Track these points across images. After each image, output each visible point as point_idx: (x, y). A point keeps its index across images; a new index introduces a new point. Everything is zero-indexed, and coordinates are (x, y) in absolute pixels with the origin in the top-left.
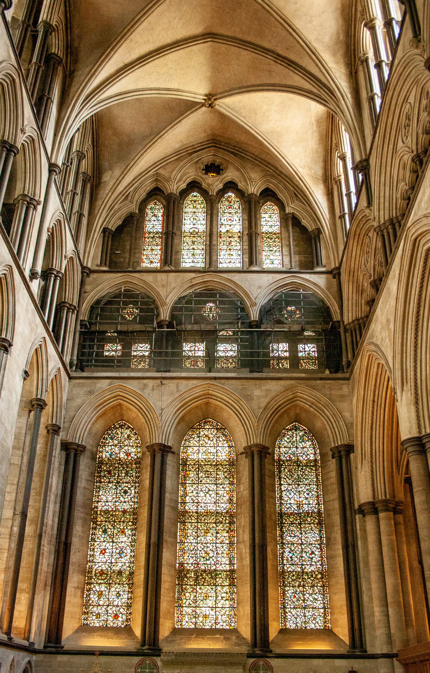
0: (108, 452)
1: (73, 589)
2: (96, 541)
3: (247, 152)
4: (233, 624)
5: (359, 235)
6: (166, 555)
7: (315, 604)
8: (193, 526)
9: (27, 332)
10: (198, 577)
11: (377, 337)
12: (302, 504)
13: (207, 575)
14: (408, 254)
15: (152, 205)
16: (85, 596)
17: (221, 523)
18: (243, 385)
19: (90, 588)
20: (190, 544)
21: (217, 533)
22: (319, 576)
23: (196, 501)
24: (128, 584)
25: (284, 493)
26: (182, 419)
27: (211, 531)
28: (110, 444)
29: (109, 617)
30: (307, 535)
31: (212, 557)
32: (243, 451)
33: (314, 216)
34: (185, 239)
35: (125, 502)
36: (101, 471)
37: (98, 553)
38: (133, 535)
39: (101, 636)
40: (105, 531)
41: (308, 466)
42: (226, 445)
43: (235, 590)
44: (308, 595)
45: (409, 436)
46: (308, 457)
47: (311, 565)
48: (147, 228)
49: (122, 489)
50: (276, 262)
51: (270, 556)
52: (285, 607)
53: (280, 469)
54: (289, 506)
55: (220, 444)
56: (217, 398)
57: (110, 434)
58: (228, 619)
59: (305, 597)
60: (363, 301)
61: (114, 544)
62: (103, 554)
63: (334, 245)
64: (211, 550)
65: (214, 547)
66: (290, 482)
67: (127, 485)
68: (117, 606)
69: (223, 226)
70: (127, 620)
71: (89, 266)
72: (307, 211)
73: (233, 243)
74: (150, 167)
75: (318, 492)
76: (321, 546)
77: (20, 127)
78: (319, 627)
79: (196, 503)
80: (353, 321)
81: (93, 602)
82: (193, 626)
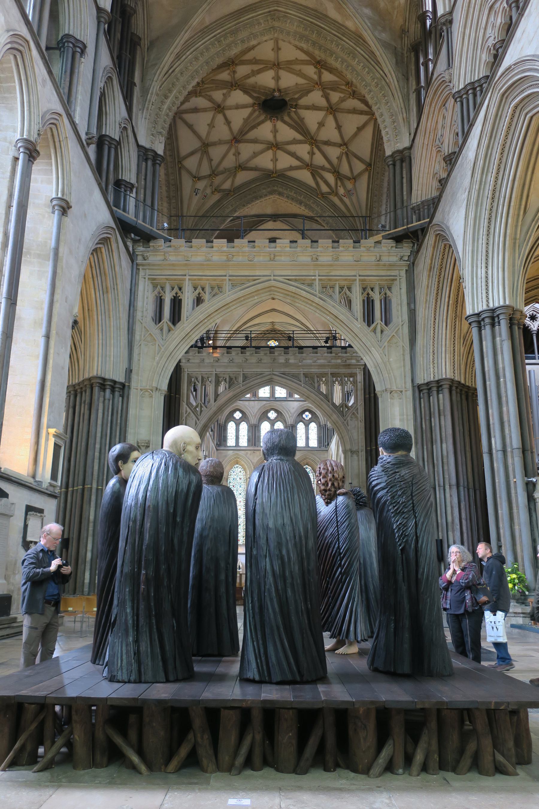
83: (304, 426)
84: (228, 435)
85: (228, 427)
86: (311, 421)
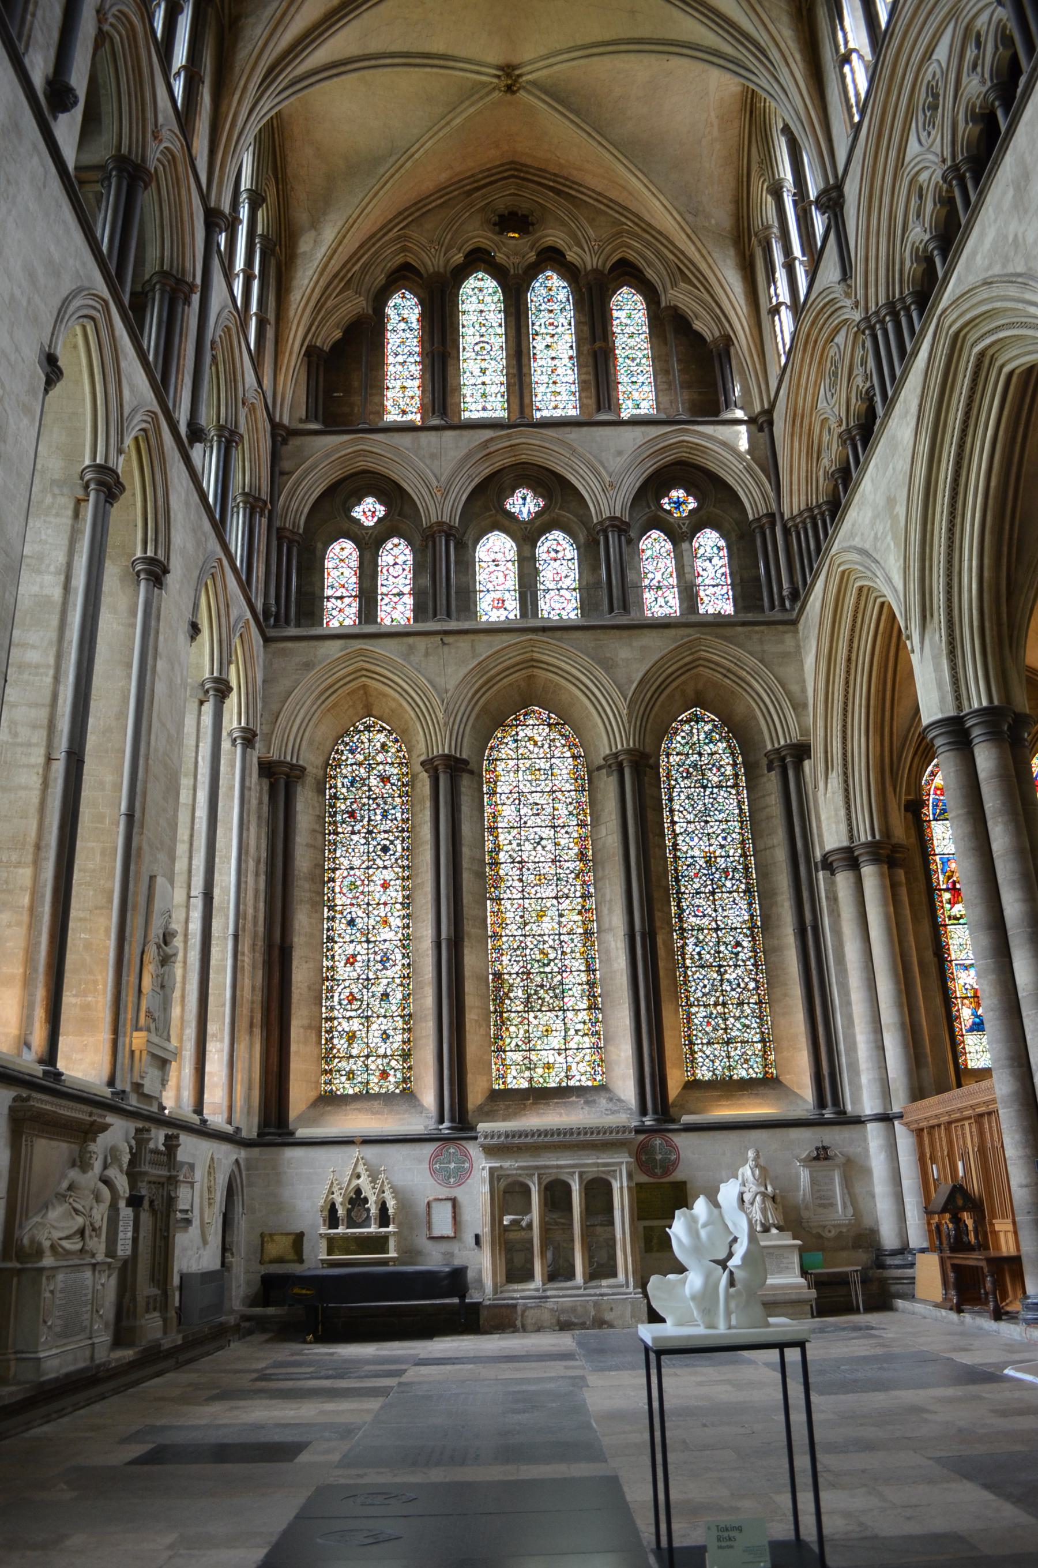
0: (346, 777)
1: (302, 1030)
2: (336, 942)
3: (581, 185)
4: (599, 1078)
5: (816, 342)
6: (470, 960)
7: (746, 1035)
8: (516, 906)
9: (190, 547)
10: (529, 996)
11: (862, 534)
12: (716, 857)
13: (546, 992)
14: (940, 362)
15: (396, 300)
16: (323, 1042)
17: (567, 897)
18: (596, 640)
19: (331, 1027)
20: (511, 939)
21: (561, 916)
22: (752, 985)
23: (519, 859)
24: (402, 1017)
25: (680, 838)
26: (484, 710)
27: (549, 913)
28: (349, 762)
29: (371, 1077)
30: (725, 914)
31: (553, 960)
32: (602, 762)
33: (718, 311)
34: (465, 365)
35: (385, 867)
36: (335, 813)
37: (342, 964)
38: (404, 928)
39: (359, 1110)
40: (351, 923)
41: (722, 787)
42: (568, 754)
43: (600, 1016)
44: (732, 1020)
45: (940, 716)
46: (723, 770)
47: (736, 966)
48: (389, 346)
49: (379, 844)
50: (644, 404)
51: (661, 952)
52: (691, 1043)
53: (671, 794)
54: (690, 860)
55: (557, 753)
57: (347, 744)
58: (589, 1069)
59: (728, 1023)
60: (821, 473)
61: (371, 946)
62: (352, 964)
63: (758, 366)
64: (551, 947)
65: (557, 942)
66: (690, 817)
67: (386, 836)
68: (385, 1056)
69: (539, 338)
70: (405, 1080)
71: (286, 421)
72: (701, 302)
73: (559, 371)
74: (391, 221)
75: (743, 835)
76: (752, 932)
77: (150, 128)
78: (754, 1076)
79: (519, 862)
80: (800, 514)
81: (338, 1051)
82: (525, 1085)
83: (669, 546)
84: (328, 592)
85: (329, 564)
86: (698, 523)
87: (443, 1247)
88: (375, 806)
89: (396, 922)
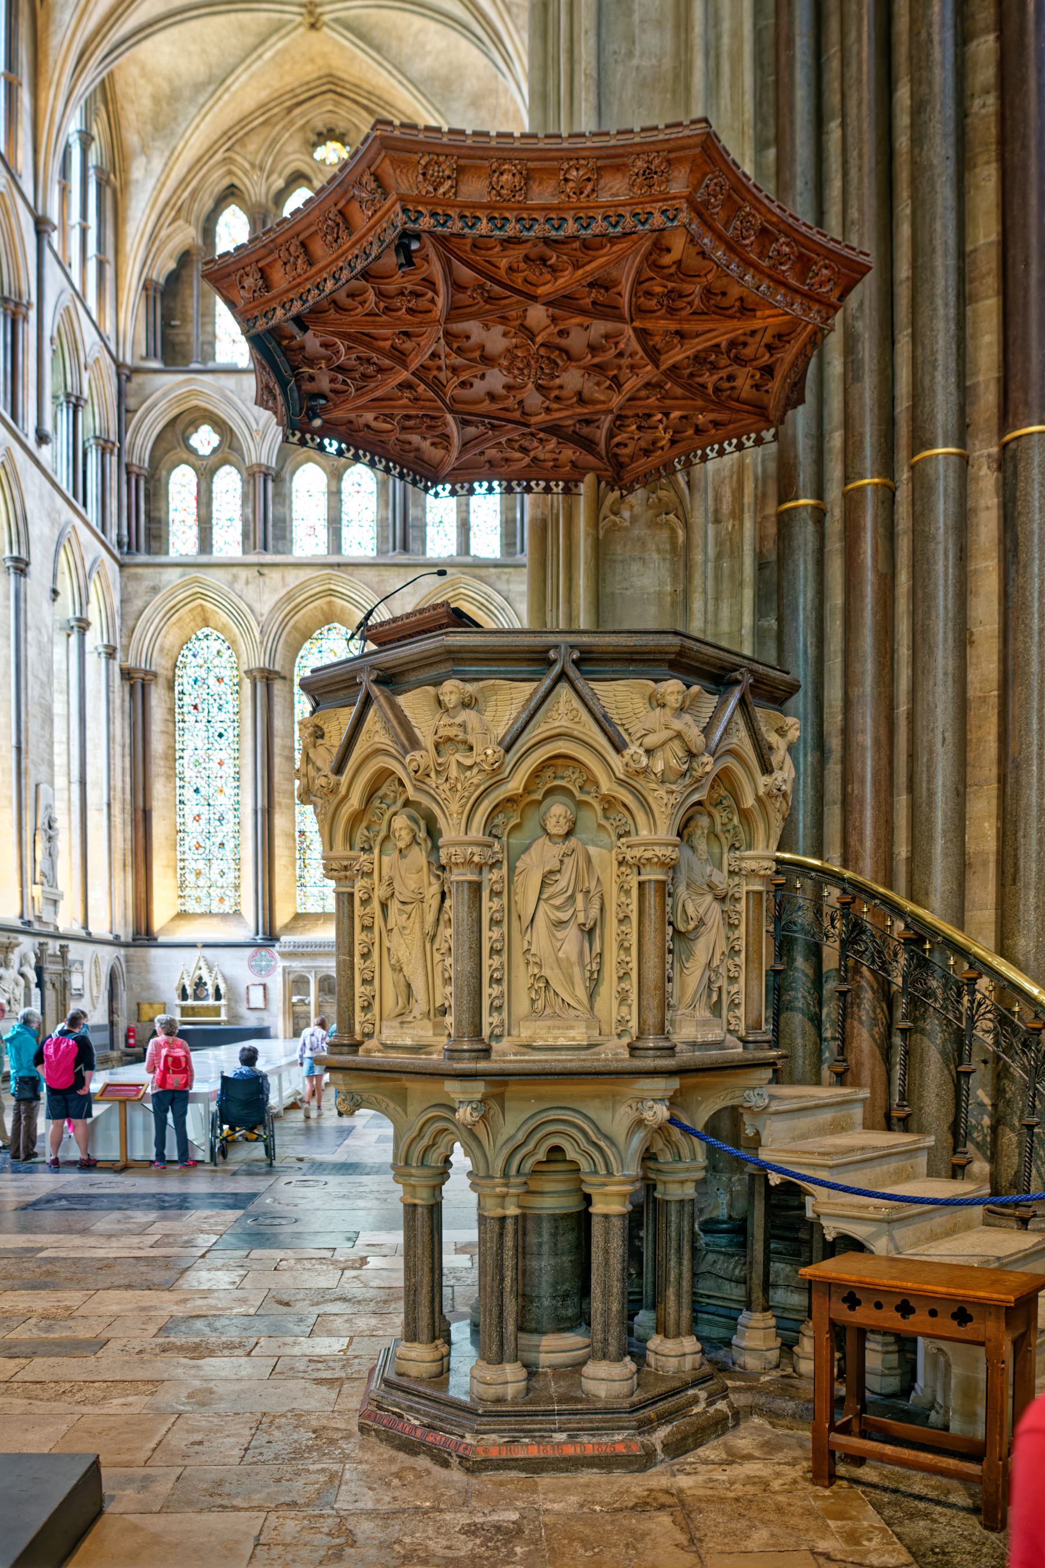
40: (197, 791)
56: (342, 596)
87: (257, 1014)
88: (212, 701)
89: (229, 791)
